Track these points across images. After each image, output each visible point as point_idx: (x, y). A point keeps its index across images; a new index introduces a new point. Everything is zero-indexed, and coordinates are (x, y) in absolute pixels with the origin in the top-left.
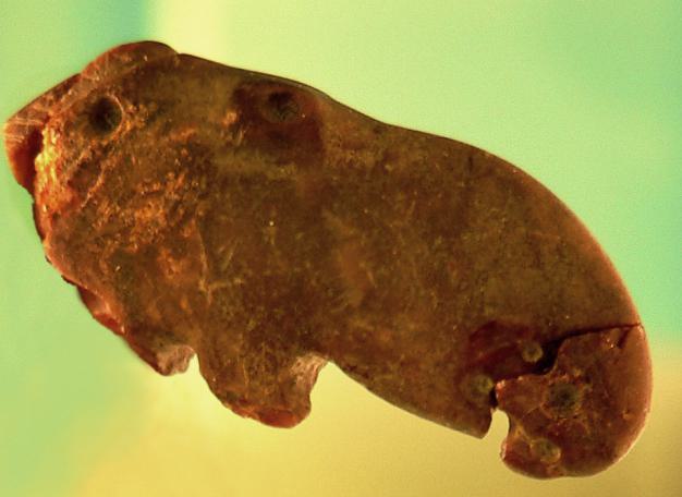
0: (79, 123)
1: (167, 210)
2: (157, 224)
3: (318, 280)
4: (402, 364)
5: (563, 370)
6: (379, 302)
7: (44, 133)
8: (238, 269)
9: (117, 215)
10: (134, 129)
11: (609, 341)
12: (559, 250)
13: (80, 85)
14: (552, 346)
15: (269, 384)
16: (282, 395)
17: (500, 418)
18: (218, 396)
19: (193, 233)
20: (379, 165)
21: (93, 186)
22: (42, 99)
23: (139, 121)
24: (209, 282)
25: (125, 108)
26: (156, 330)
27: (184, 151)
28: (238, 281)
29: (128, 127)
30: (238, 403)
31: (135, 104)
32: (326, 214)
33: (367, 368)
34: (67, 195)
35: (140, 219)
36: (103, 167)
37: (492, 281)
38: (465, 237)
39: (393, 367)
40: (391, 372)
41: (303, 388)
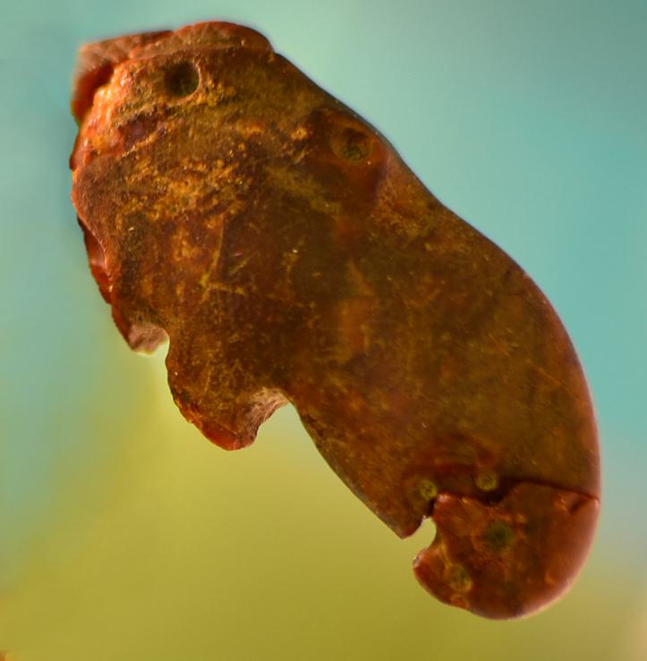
0: (154, 76)
1: (202, 196)
2: (186, 204)
3: (316, 323)
4: (360, 437)
5: (509, 510)
6: (365, 371)
7: (117, 71)
8: (243, 279)
9: (152, 178)
10: (204, 104)
11: (564, 503)
12: (553, 396)
13: (171, 40)
14: (509, 482)
15: (226, 400)
16: (234, 417)
17: (428, 528)
18: (173, 391)
19: (217, 228)
20: (418, 243)
21: (141, 141)
22: (128, 40)
23: (212, 100)
24: (211, 280)
25: (204, 81)
26: (142, 303)
27: (242, 147)
28: (240, 291)
29: (199, 100)
30: (189, 405)
31: (216, 82)
32: (351, 265)
33: (324, 426)
34: (113, 139)
35: (172, 191)
36: (159, 128)
37: (480, 397)
38: (472, 345)
39: (350, 436)
40: (346, 441)
41: (256, 417)
